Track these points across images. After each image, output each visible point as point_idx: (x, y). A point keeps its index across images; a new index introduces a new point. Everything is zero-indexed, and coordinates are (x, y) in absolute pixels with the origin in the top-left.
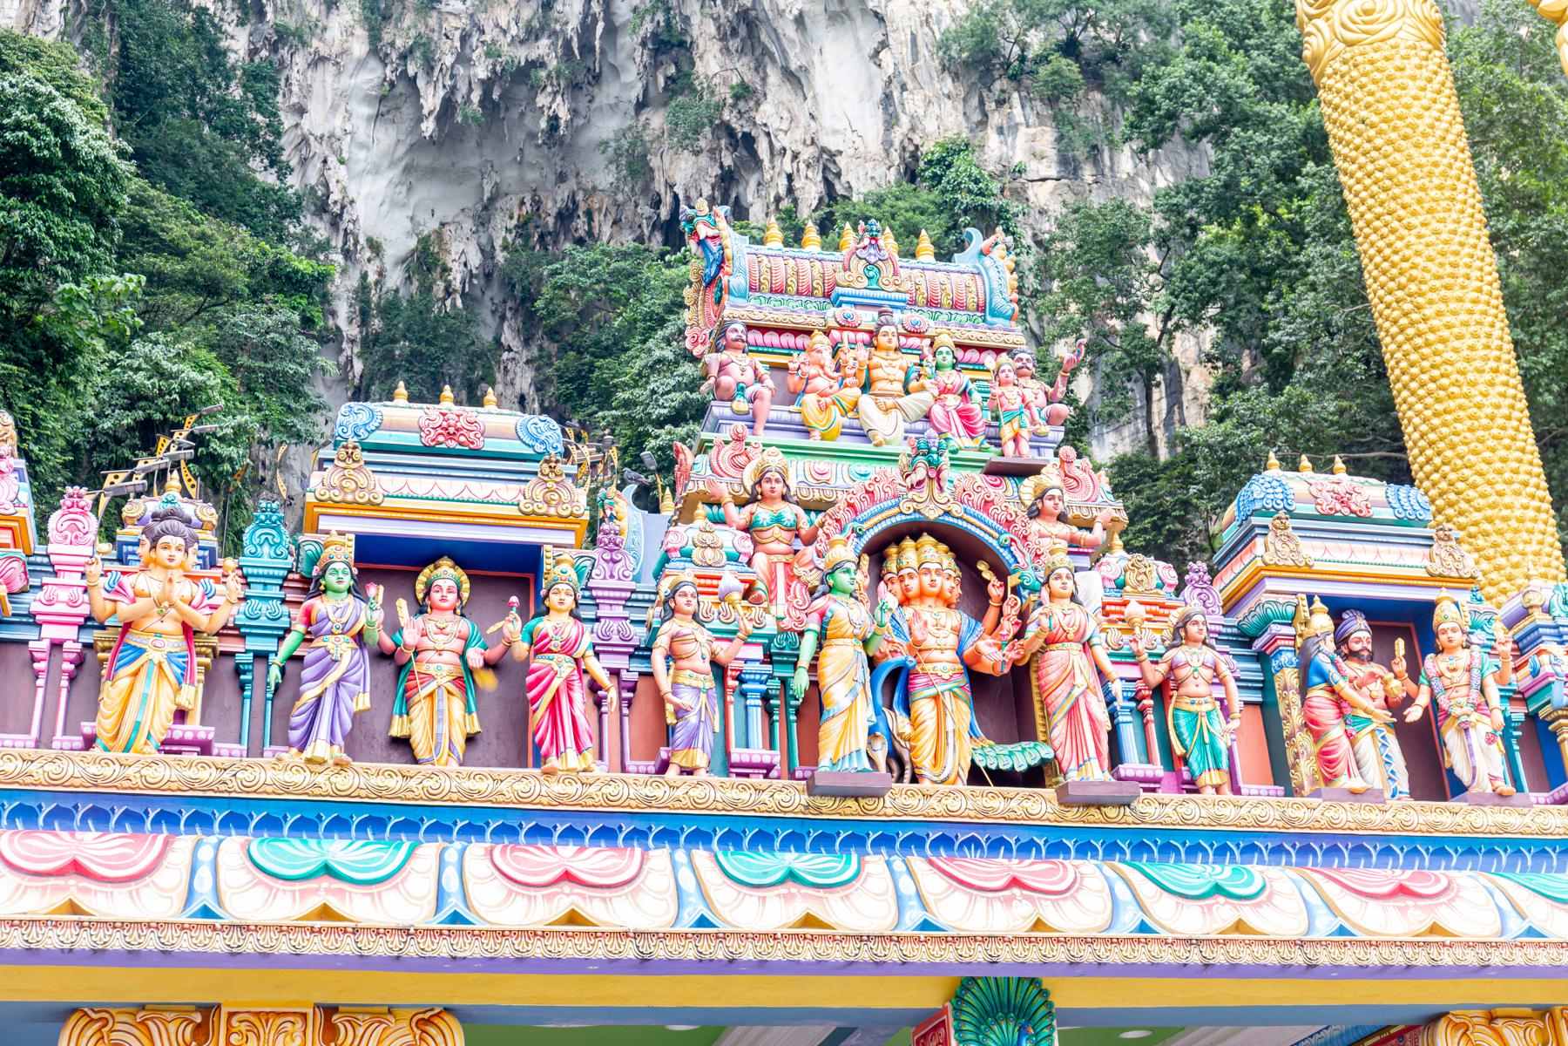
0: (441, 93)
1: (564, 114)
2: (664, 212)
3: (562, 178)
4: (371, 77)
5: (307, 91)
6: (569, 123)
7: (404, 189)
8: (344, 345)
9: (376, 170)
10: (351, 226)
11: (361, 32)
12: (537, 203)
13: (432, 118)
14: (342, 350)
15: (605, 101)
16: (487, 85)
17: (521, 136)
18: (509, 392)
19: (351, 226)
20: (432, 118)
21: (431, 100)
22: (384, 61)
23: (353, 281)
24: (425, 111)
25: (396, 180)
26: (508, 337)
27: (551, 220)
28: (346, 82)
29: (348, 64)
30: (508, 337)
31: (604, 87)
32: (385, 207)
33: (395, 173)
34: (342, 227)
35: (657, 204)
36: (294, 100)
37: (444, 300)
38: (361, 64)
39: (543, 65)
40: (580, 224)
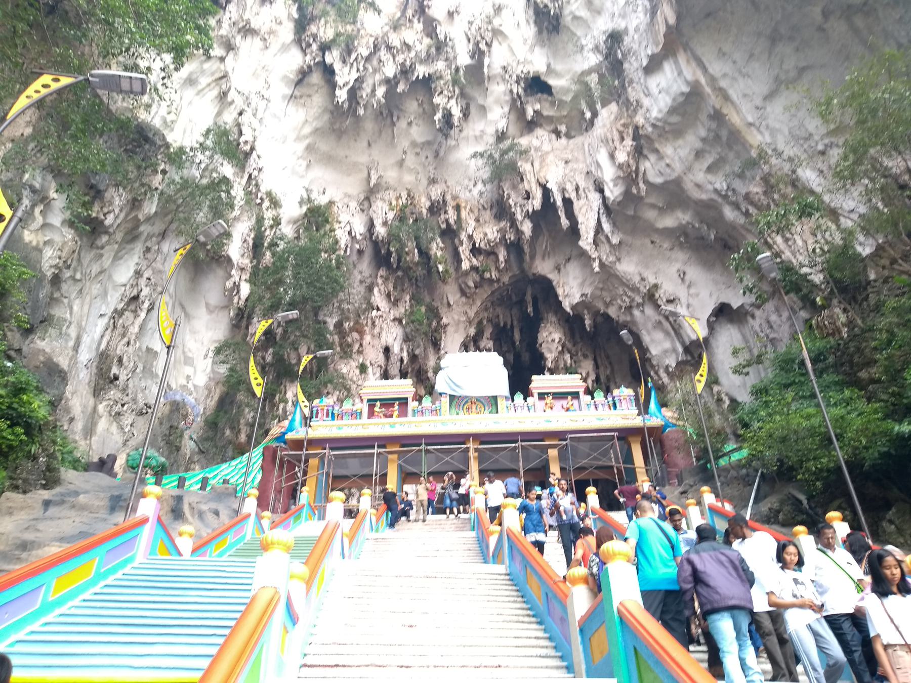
2: (536, 203)
3: (433, 181)
7: (304, 163)
8: (233, 272)
10: (255, 173)
14: (230, 276)
15: (471, 133)
17: (405, 144)
18: (376, 342)
26: (378, 298)
27: (424, 211)
29: (275, 44)
30: (378, 298)
31: (470, 124)
34: (247, 170)
35: (528, 196)
38: (285, 48)
39: (441, 77)
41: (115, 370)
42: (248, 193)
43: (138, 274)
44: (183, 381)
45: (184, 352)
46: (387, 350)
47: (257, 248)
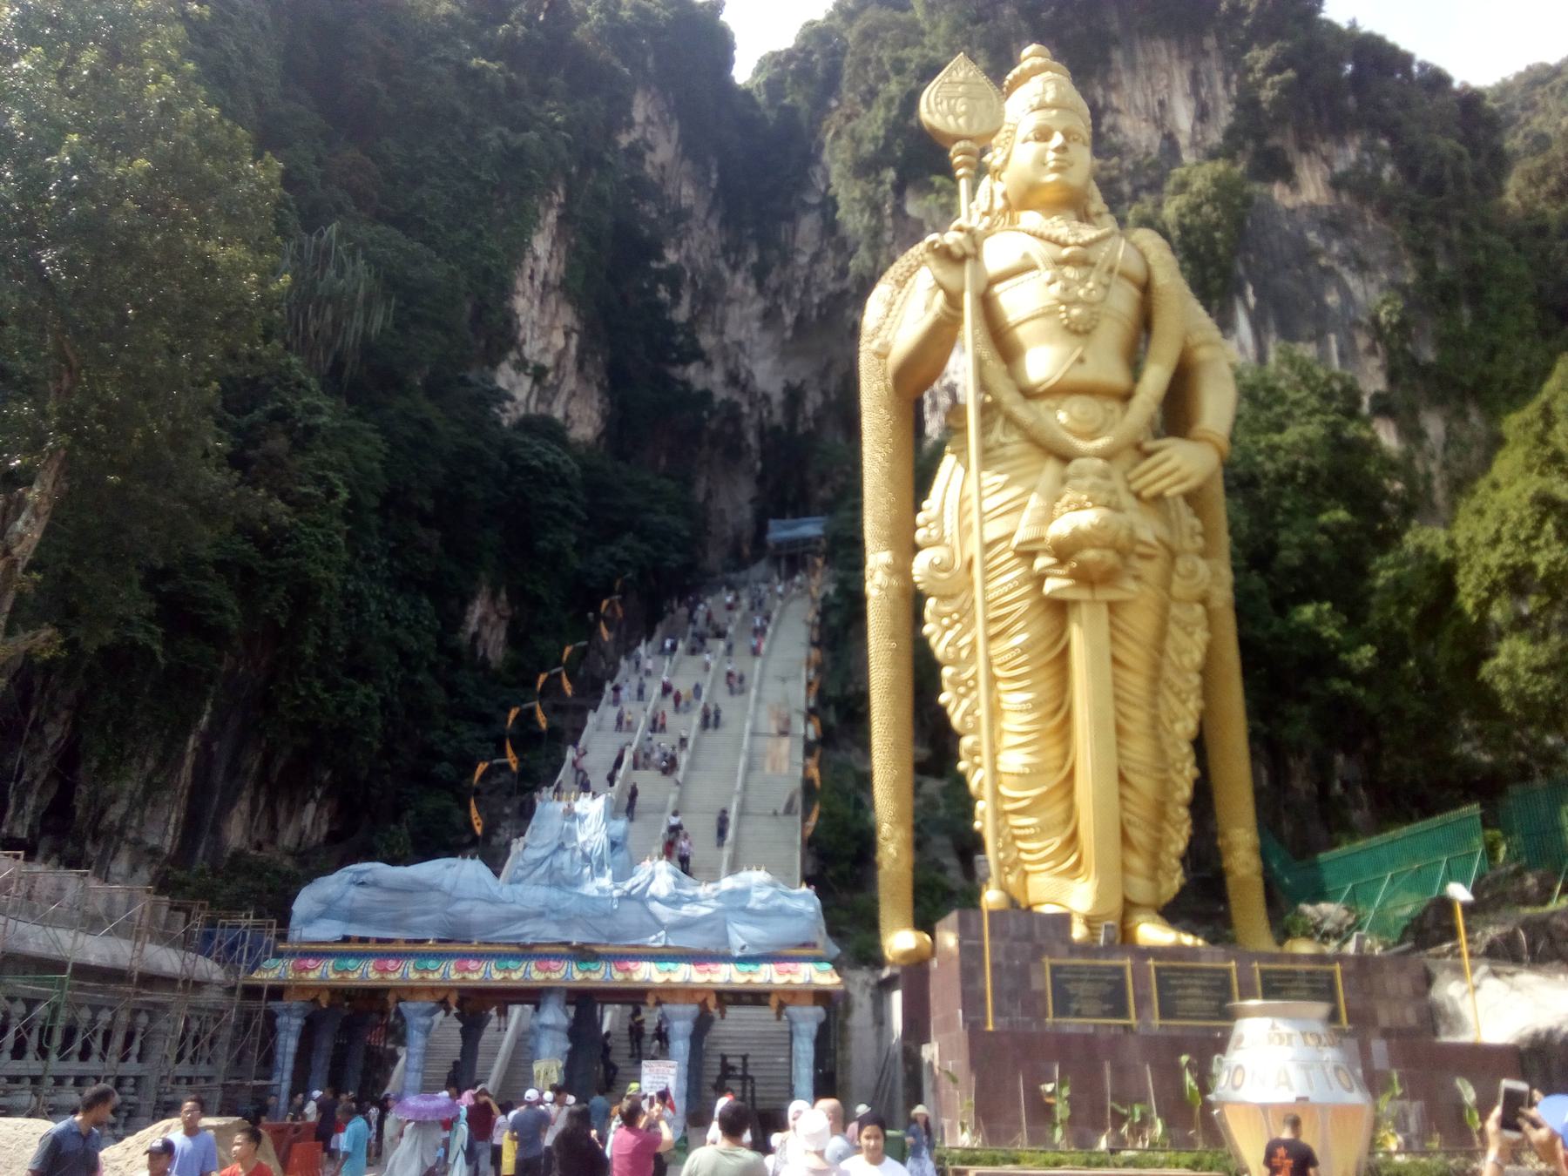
4: (758, 306)
5: (723, 320)
11: (752, 282)
16: (820, 306)
21: (789, 318)
22: (765, 296)
23: (756, 416)
28: (746, 311)
33: (775, 357)
38: (753, 301)
42: (751, 404)
47: (762, 434)
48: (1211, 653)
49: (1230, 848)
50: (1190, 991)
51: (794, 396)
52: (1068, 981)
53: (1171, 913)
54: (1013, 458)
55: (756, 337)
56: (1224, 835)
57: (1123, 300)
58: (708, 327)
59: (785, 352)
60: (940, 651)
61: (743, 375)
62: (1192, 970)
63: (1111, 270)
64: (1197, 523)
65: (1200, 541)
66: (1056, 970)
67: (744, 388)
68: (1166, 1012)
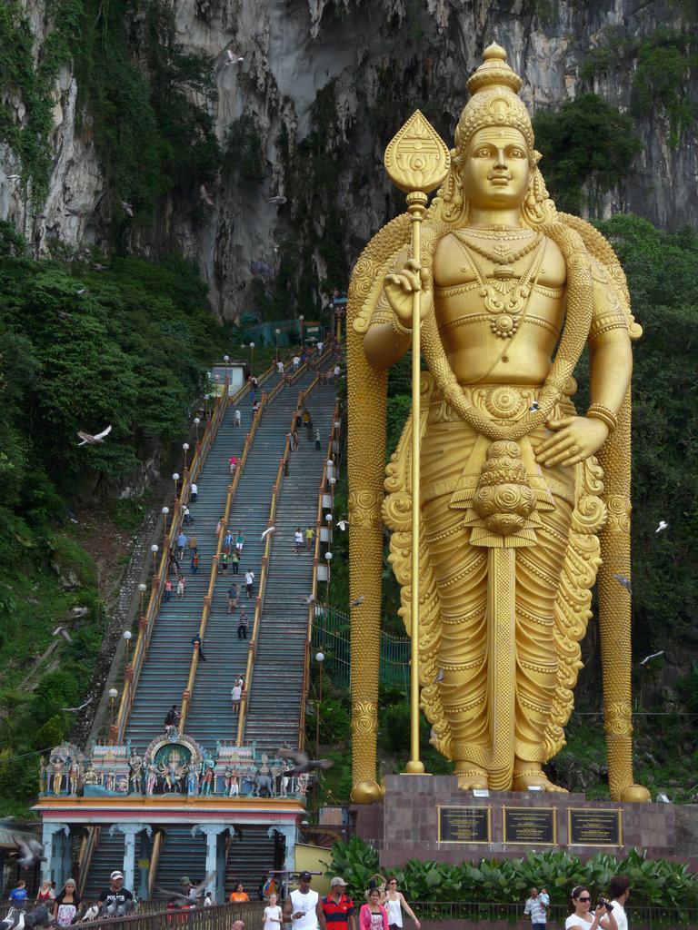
0: (323, 5)
1: (401, 13)
6: (406, 19)
7: (308, 60)
9: (288, 53)
12: (393, 62)
13: (317, 24)
19: (273, 96)
20: (317, 24)
21: (316, 12)
23: (276, 132)
24: (313, 20)
25: (302, 56)
27: (401, 75)
32: (295, 76)
33: (299, 53)
34: (268, 98)
36: (229, 26)
37: (335, 136)
40: (419, 78)
41: (224, 273)
43: (222, 211)
44: (259, 255)
45: (256, 237)
46: (387, 197)
48: (601, 572)
49: (610, 716)
50: (526, 824)
51: (325, 101)
52: (452, 819)
53: (552, 770)
54: (452, 433)
55: (276, 31)
56: (606, 707)
57: (539, 304)
58: (218, 24)
59: (311, 47)
60: (401, 575)
61: (261, 81)
62: (529, 811)
63: (532, 281)
64: (600, 470)
65: (600, 485)
66: (444, 812)
67: (262, 97)
68: (512, 836)
